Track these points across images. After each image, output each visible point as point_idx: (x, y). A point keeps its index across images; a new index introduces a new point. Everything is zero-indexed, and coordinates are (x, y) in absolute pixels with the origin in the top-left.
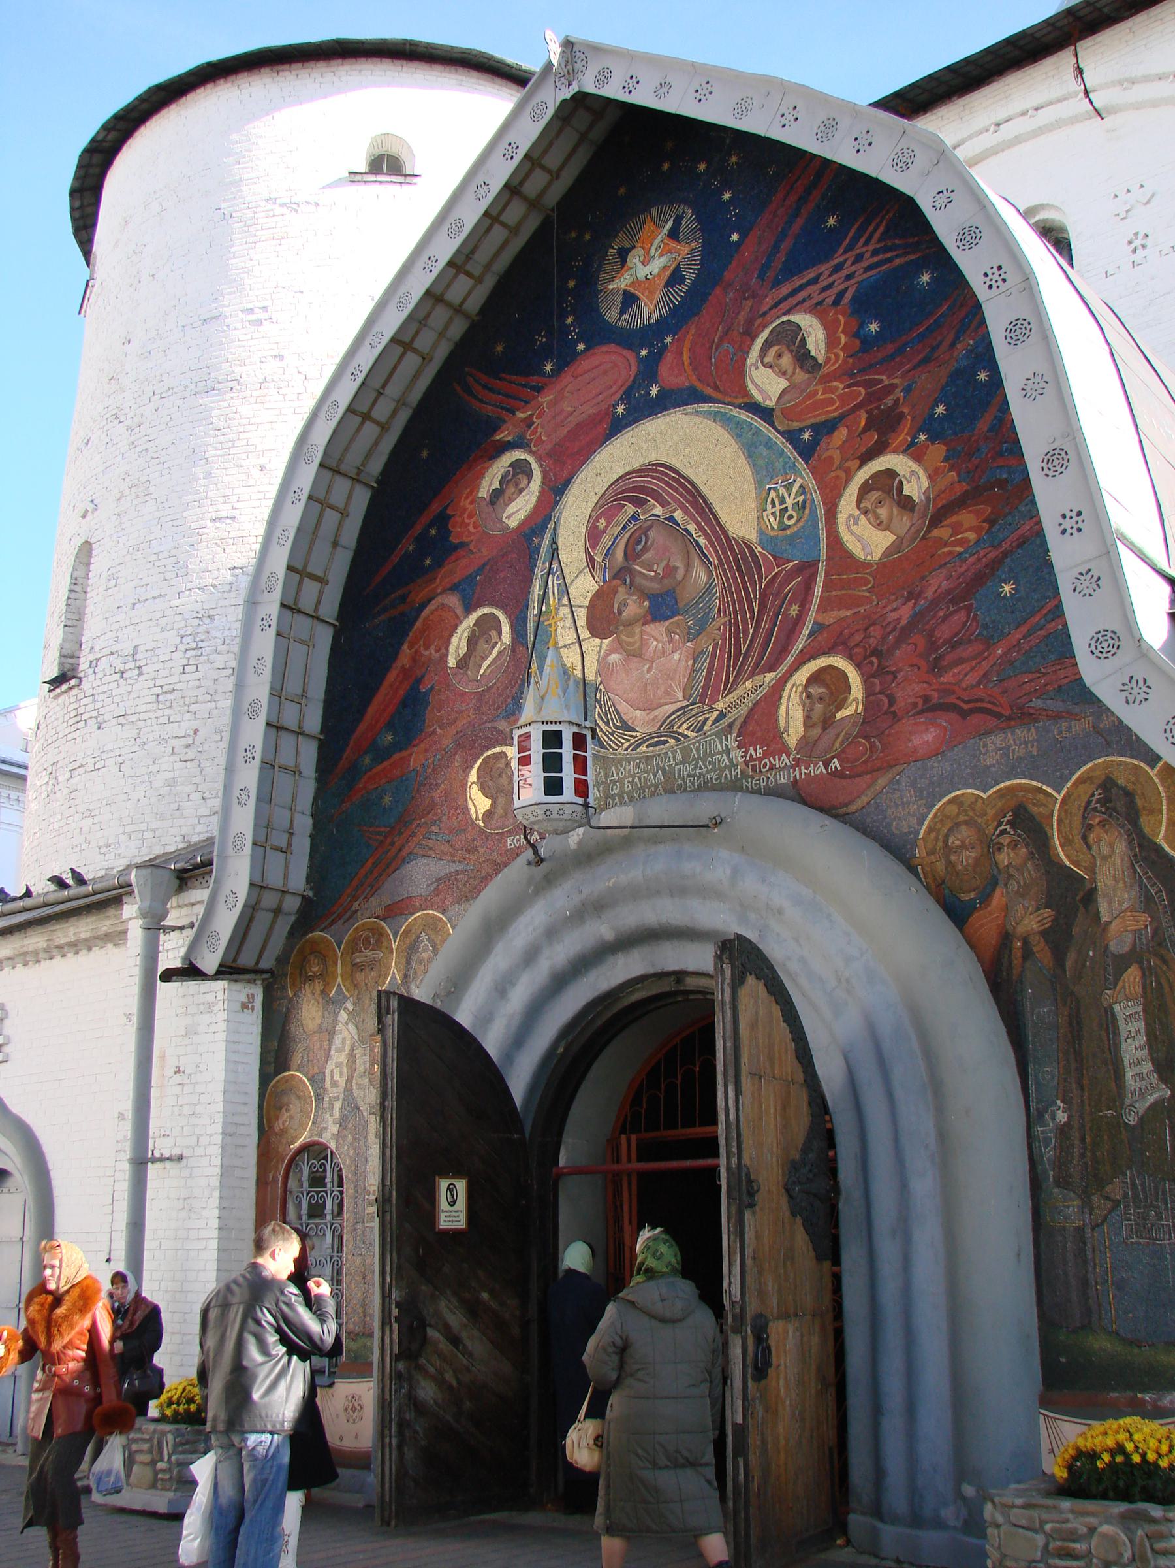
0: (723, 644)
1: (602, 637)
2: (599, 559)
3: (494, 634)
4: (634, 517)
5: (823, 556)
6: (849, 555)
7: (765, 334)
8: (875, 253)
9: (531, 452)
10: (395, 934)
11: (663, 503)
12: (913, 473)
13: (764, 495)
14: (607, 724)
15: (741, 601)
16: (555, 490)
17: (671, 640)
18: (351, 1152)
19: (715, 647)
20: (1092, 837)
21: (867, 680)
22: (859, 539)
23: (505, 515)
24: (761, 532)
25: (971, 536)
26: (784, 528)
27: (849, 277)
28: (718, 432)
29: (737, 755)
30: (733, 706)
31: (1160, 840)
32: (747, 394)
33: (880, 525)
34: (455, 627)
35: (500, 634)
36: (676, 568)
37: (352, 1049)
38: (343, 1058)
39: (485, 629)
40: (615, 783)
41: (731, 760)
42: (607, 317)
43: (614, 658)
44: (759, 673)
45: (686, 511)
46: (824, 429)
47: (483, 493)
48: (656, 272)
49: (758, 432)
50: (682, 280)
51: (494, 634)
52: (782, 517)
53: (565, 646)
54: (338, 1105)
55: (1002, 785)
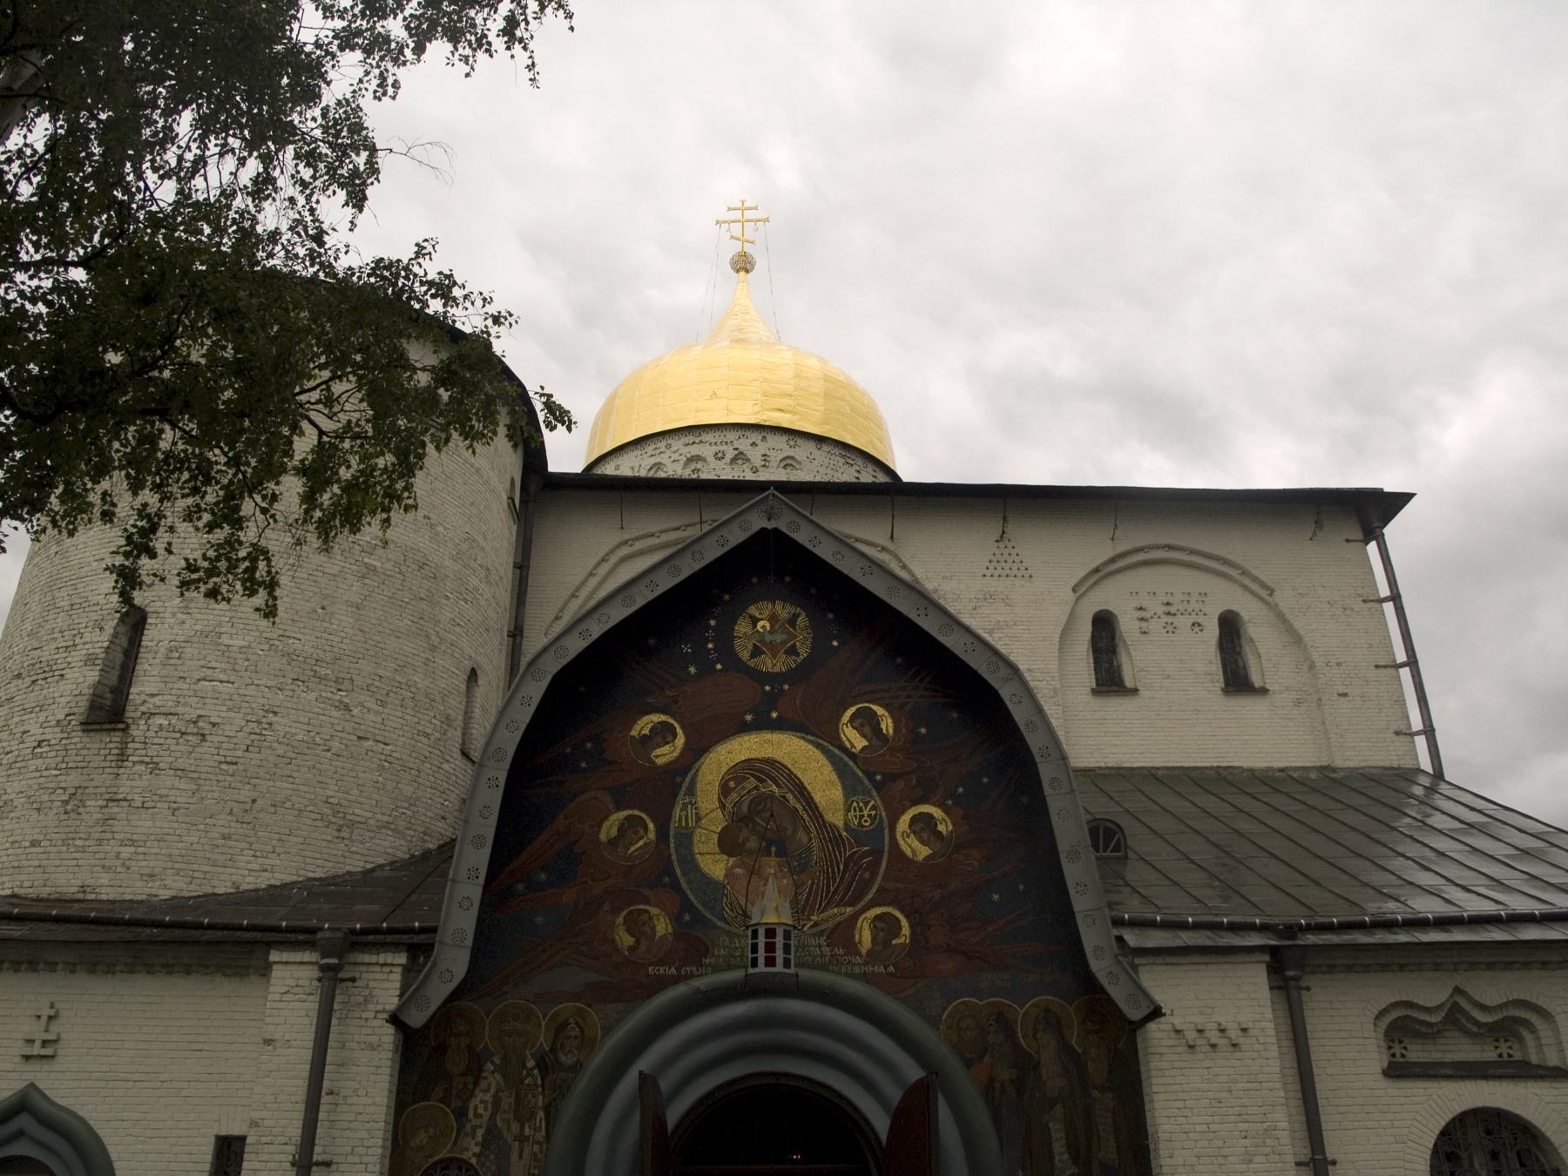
0: (818, 883)
1: (730, 855)
2: (729, 806)
3: (641, 832)
4: (756, 788)
5: (886, 848)
6: (903, 854)
7: (853, 709)
8: (926, 689)
9: (675, 719)
10: (544, 1017)
11: (778, 786)
12: (943, 819)
13: (849, 802)
14: (732, 910)
15: (831, 861)
16: (697, 750)
17: (781, 871)
18: (493, 1168)
19: (813, 883)
20: (1038, 1036)
21: (911, 926)
22: (910, 847)
23: (654, 754)
24: (846, 824)
25: (976, 863)
26: (860, 825)
27: (909, 697)
28: (818, 754)
29: (826, 950)
30: (826, 920)
31: (1073, 1042)
32: (839, 739)
33: (923, 842)
34: (606, 817)
35: (646, 833)
36: (787, 829)
37: (498, 1091)
38: (488, 1097)
39: (631, 827)
40: (737, 948)
41: (822, 952)
42: (740, 655)
43: (738, 870)
44: (843, 905)
45: (795, 796)
46: (890, 778)
47: (634, 733)
48: (778, 641)
49: (846, 765)
50: (798, 654)
51: (641, 832)
52: (860, 821)
53: (700, 854)
54: (480, 1133)
55: (991, 1000)
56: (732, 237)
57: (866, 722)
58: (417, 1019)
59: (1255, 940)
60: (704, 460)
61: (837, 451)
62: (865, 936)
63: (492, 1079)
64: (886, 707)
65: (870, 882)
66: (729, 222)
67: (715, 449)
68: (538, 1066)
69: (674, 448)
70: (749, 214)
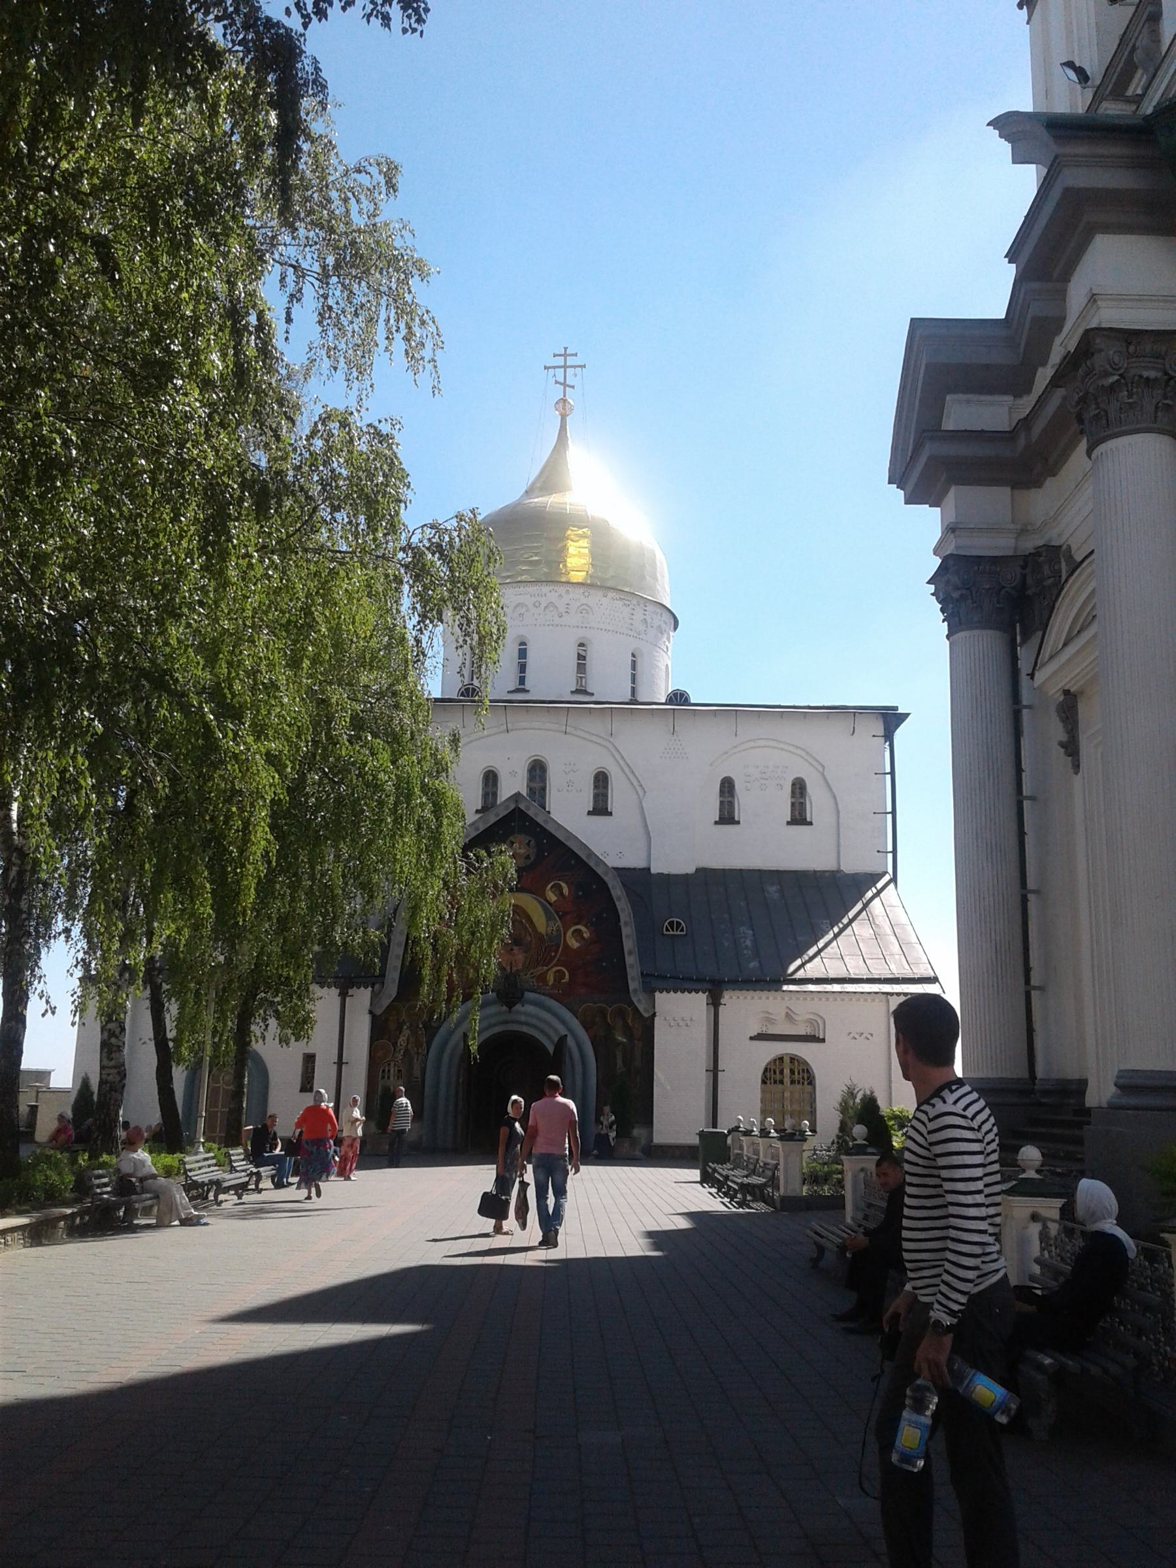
28: (536, 903)
54: (402, 1052)
56: (557, 382)
57: (557, 889)
58: (379, 1012)
59: (706, 986)
60: (526, 606)
61: (618, 596)
62: (551, 978)
63: (406, 1032)
64: (567, 883)
65: (555, 955)
66: (555, 367)
67: (534, 599)
68: (424, 1026)
70: (571, 361)
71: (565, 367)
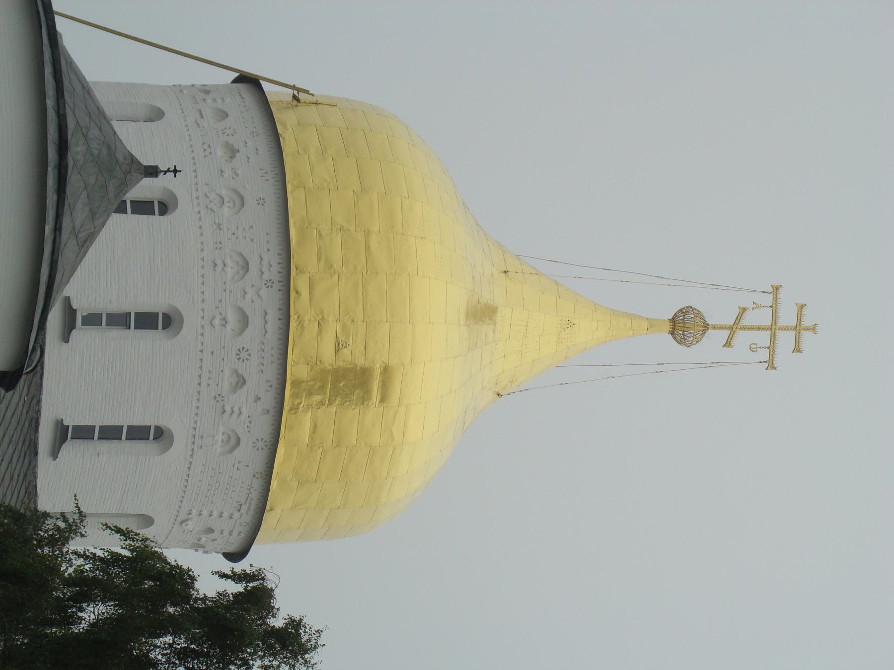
66: (774, 307)
69: (264, 292)
70: (786, 340)
71: (773, 328)
